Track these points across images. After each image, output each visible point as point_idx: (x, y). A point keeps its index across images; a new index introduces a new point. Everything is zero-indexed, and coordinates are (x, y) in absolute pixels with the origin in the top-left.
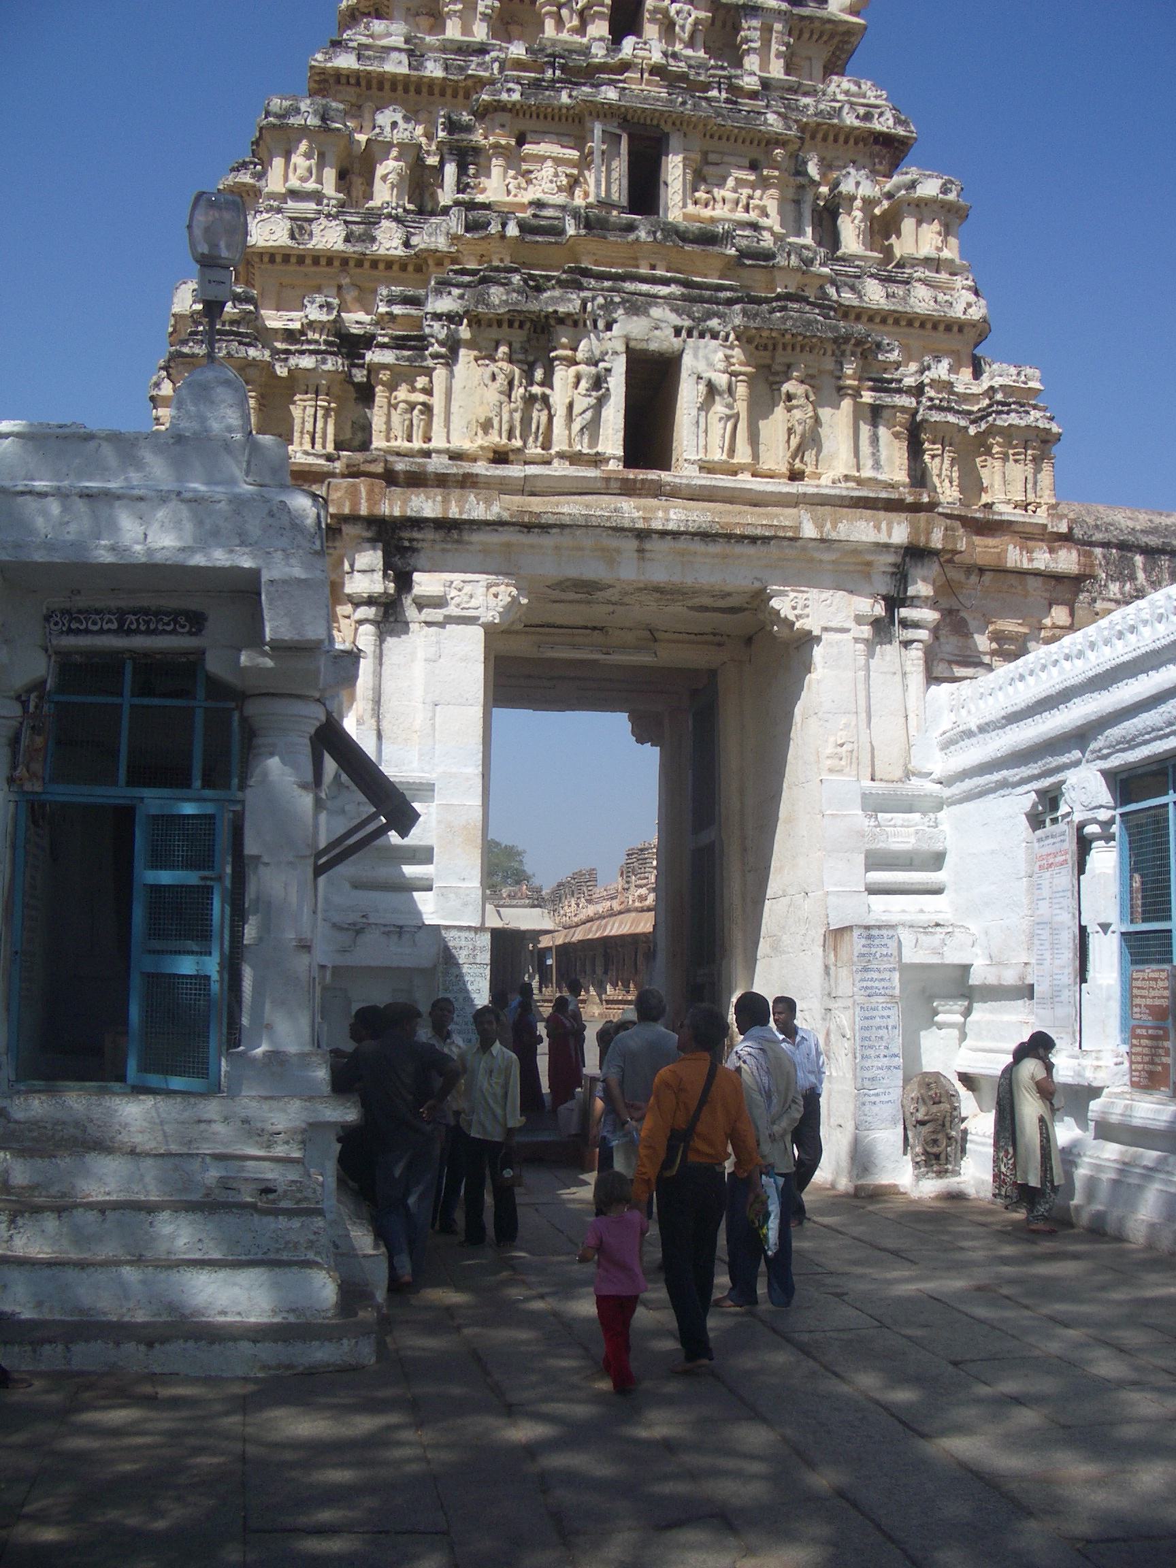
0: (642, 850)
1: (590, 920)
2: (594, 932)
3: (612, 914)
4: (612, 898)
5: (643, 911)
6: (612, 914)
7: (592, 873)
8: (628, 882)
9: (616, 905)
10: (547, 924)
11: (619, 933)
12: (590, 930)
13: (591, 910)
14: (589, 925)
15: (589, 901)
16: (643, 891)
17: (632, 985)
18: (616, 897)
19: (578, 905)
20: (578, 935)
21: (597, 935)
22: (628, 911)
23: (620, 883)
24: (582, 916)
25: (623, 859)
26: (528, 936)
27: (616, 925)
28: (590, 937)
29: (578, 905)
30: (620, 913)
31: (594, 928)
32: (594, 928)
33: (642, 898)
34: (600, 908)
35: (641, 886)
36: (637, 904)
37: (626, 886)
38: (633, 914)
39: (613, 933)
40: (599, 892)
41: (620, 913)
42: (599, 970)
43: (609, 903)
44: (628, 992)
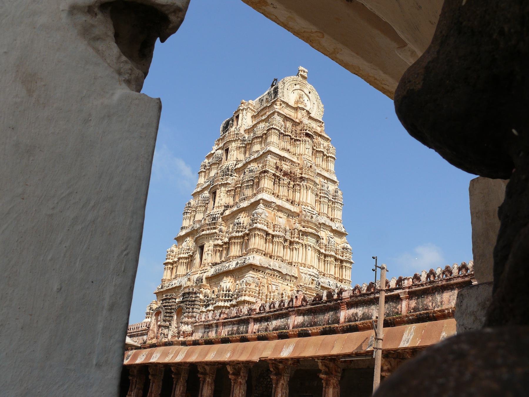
35: (187, 324)
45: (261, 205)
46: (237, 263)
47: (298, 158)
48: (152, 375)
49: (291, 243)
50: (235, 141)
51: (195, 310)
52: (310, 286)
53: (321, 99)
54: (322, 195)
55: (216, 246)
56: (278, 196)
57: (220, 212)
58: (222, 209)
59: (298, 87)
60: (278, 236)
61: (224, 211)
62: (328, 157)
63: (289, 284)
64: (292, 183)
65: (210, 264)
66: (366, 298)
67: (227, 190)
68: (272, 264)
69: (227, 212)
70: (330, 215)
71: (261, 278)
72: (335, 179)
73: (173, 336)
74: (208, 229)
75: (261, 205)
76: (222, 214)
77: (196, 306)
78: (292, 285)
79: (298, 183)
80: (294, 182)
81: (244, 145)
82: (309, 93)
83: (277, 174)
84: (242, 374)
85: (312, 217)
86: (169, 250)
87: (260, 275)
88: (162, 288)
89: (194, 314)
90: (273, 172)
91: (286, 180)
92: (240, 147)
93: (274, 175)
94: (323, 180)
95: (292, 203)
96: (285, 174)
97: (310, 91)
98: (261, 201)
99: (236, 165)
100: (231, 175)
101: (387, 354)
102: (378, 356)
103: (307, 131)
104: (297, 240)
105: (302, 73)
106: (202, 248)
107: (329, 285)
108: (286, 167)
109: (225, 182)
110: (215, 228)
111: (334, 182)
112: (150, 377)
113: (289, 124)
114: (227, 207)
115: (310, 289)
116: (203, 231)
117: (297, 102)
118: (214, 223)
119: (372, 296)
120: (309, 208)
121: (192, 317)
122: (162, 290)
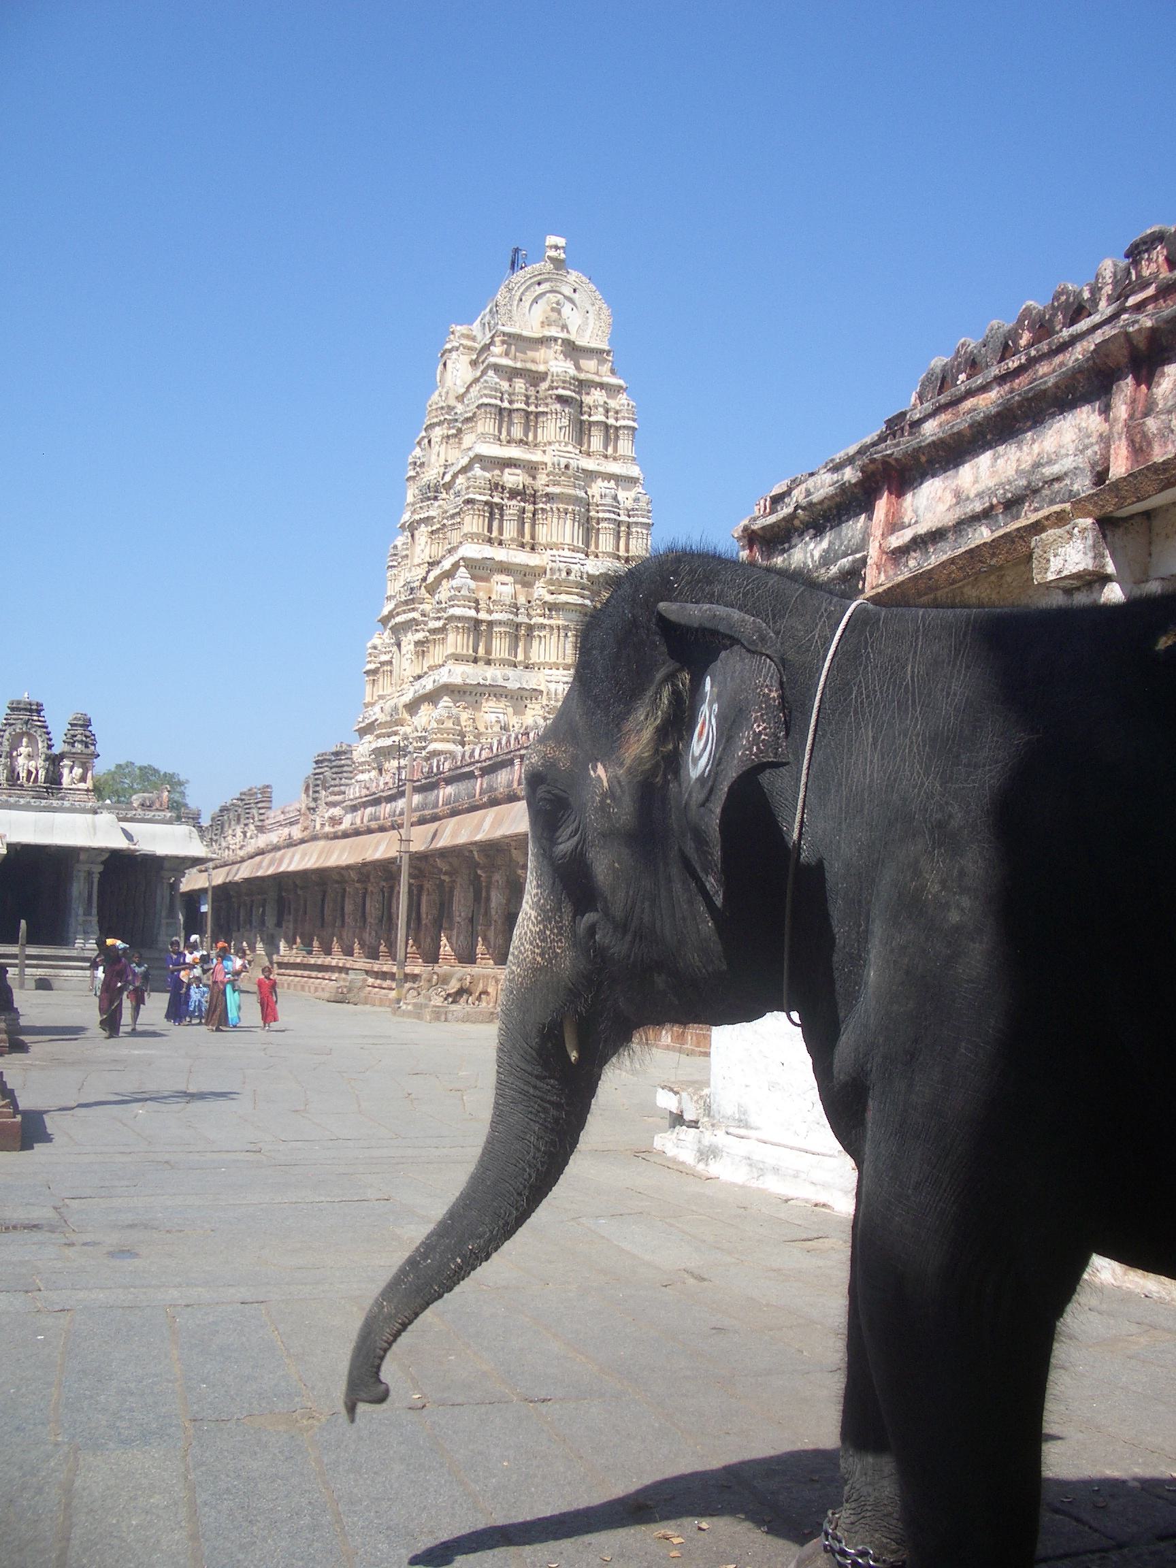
0: (337, 754)
1: (261, 852)
2: (266, 868)
3: (291, 844)
4: (291, 824)
5: (336, 837)
6: (291, 844)
7: (266, 790)
8: (315, 800)
10: (197, 849)
11: (301, 867)
12: (259, 865)
13: (262, 841)
14: (258, 858)
15: (261, 829)
16: (336, 811)
17: (316, 943)
18: (297, 822)
19: (245, 833)
20: (244, 872)
21: (269, 872)
22: (315, 838)
23: (303, 801)
24: (250, 848)
25: (310, 768)
26: (167, 865)
28: (259, 874)
29: (245, 833)
30: (303, 841)
31: (265, 863)
32: (265, 863)
33: (334, 821)
34: (273, 838)
36: (327, 829)
37: (312, 805)
38: (322, 843)
39: (292, 868)
40: (274, 815)
41: (303, 841)
42: (270, 921)
43: (286, 831)
44: (310, 952)
45: (462, 569)
47: (544, 452)
49: (530, 628)
50: (440, 424)
53: (604, 298)
54: (601, 515)
55: (417, 643)
56: (500, 543)
57: (420, 577)
58: (421, 572)
59: (546, 286)
60: (500, 623)
61: (428, 572)
62: (617, 429)
64: (530, 507)
66: (459, 771)
67: (430, 529)
68: (489, 676)
69: (430, 579)
70: (622, 553)
72: (635, 471)
74: (404, 612)
75: (462, 569)
76: (424, 579)
79: (541, 505)
80: (534, 503)
81: (454, 431)
82: (575, 291)
83: (496, 500)
84: (372, 880)
85: (568, 574)
86: (369, 645)
90: (484, 498)
91: (513, 506)
92: (448, 437)
93: (486, 503)
94: (606, 484)
95: (533, 549)
96: (514, 494)
97: (576, 286)
98: (462, 563)
99: (444, 474)
100: (436, 498)
102: (406, 858)
103: (561, 392)
104: (541, 620)
105: (552, 253)
106: (399, 645)
108: (513, 478)
109: (426, 515)
110: (413, 610)
111: (633, 481)
112: (300, 892)
113: (520, 384)
114: (432, 564)
116: (398, 614)
117: (547, 323)
118: (413, 600)
119: (467, 769)
120: (567, 553)
122: (362, 725)
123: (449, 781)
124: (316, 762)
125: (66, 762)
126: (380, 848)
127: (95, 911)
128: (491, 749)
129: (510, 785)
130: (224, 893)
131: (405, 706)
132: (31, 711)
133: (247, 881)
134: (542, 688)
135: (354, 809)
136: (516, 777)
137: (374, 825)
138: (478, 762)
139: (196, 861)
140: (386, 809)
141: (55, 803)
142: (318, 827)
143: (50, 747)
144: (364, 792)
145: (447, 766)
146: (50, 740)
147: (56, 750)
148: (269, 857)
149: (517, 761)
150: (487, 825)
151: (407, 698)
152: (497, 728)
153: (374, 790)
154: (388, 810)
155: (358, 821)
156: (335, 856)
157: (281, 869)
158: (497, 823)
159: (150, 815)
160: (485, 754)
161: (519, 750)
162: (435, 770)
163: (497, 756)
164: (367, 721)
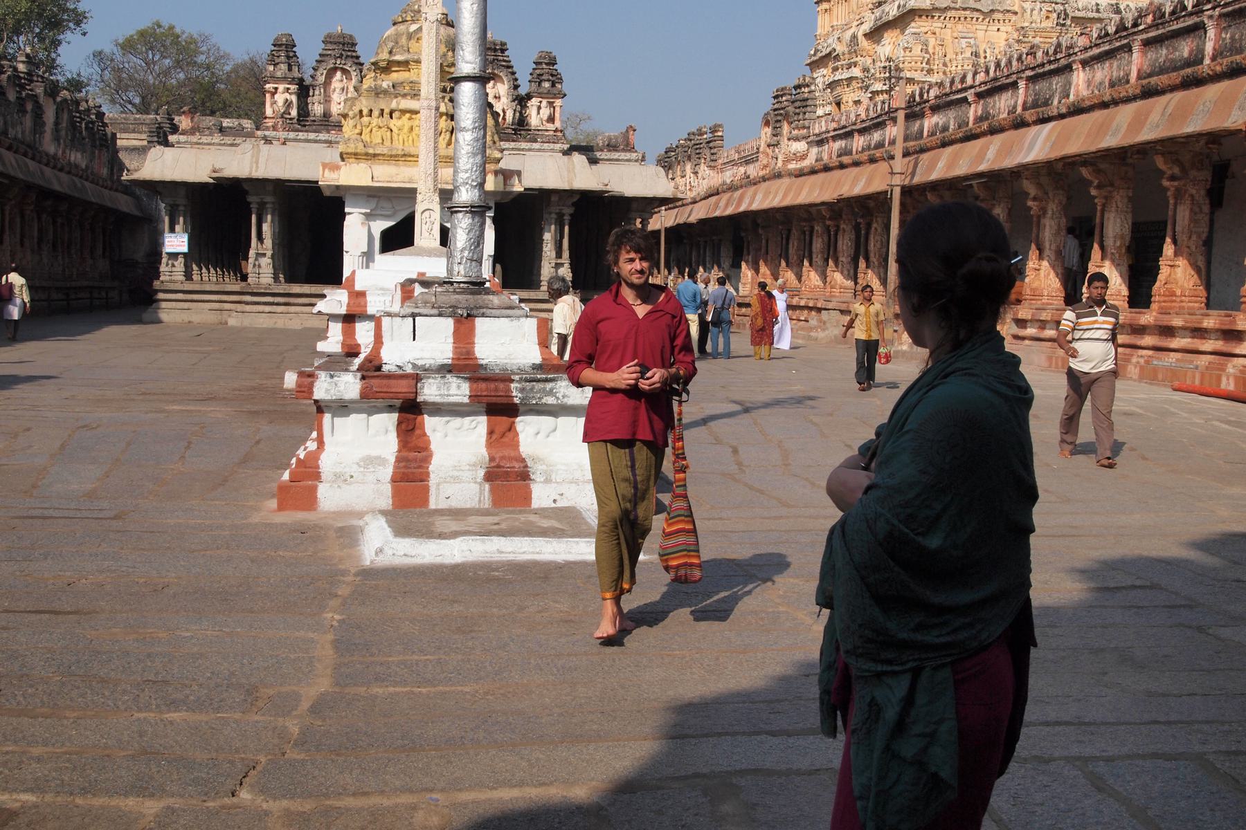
0: (797, 87)
2: (724, 208)
3: (750, 182)
4: (747, 162)
6: (750, 182)
9: (753, 171)
11: (766, 205)
12: (716, 205)
14: (713, 199)
20: (698, 213)
21: (729, 212)
22: (778, 176)
25: (768, 104)
27: (759, 197)
28: (717, 214)
30: (764, 179)
31: (722, 204)
32: (722, 204)
34: (728, 176)
35: (797, 139)
36: (792, 166)
38: (786, 181)
39: (755, 207)
41: (764, 179)
43: (742, 169)
46: (899, 7)
48: (763, 227)
51: (807, 116)
52: (1043, 25)
63: (1002, 29)
65: (871, 6)
71: (937, 31)
73: (787, 161)
77: (809, 109)
78: (1010, 29)
87: (936, 25)
88: (816, 51)
89: (806, 123)
101: (907, 191)
102: (897, 191)
107: (1098, 11)
115: (1044, 30)
121: (804, 127)
123: (935, 109)
124: (775, 97)
125: (534, 102)
126: (856, 184)
127: (566, 254)
128: (987, 72)
129: (1012, 111)
130: (677, 234)
131: (865, 35)
132: (495, 50)
133: (702, 222)
134: (1016, 8)
135: (820, 143)
136: (1020, 102)
137: (846, 160)
138: (972, 87)
139: (664, 201)
140: (859, 142)
141: (524, 145)
142: (780, 164)
143: (516, 87)
144: (834, 125)
145: (932, 94)
146: (516, 80)
147: (523, 91)
148: (725, 197)
149: (1022, 84)
150: (991, 154)
151: (866, 27)
152: (968, 54)
153: (843, 123)
154: (861, 143)
155: (825, 157)
156: (804, 193)
157: (742, 209)
158: (1005, 151)
159: (616, 155)
160: (981, 77)
161: (1023, 71)
162: (917, 98)
163: (995, 79)
164: (820, 55)
